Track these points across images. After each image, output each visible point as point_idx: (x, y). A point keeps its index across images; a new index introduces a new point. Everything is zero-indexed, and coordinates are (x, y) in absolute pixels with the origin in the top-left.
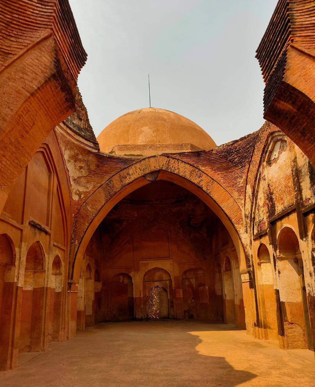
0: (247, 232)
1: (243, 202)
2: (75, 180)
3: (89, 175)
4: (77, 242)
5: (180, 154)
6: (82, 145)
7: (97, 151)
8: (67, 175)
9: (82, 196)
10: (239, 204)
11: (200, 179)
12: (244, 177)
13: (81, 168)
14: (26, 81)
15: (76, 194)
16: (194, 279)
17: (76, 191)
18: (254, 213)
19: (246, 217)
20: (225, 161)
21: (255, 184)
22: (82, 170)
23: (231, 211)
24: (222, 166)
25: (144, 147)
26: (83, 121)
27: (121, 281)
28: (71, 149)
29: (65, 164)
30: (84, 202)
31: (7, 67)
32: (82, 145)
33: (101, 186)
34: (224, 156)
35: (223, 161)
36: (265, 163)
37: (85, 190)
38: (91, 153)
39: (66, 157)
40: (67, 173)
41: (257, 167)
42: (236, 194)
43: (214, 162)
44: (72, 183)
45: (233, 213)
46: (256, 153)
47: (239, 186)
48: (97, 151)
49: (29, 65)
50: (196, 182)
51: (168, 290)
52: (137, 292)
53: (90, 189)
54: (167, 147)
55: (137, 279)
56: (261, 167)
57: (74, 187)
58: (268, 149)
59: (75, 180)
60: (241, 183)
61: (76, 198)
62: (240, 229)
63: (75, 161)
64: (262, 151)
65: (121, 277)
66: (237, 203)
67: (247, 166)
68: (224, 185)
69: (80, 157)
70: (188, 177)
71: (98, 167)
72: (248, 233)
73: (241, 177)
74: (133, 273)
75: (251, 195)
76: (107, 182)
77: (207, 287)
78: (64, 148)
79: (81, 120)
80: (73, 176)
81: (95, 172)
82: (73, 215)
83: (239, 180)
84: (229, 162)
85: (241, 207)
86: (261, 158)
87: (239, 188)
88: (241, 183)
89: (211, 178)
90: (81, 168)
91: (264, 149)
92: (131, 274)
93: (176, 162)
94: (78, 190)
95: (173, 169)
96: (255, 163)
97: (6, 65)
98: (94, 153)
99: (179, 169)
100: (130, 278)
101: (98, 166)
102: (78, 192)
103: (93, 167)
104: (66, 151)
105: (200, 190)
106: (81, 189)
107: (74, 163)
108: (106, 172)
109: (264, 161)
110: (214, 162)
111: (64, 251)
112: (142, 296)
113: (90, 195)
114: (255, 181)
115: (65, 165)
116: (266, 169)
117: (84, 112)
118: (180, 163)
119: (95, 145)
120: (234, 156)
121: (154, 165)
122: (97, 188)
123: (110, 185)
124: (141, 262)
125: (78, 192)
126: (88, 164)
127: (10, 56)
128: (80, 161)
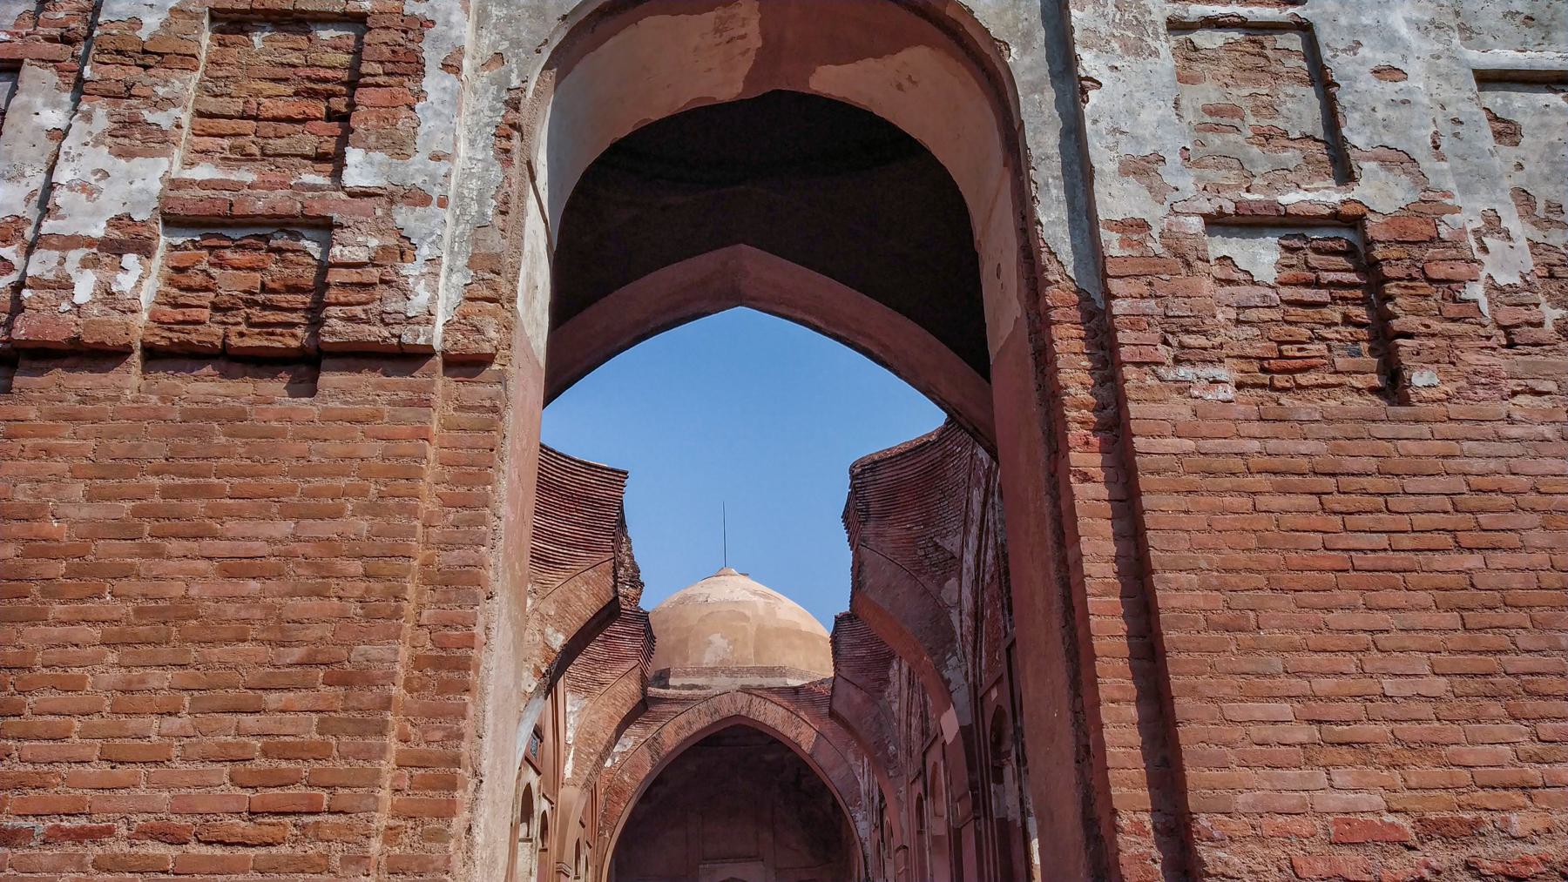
5: (769, 689)
25: (713, 671)
42: (851, 758)
50: (791, 735)
54: (749, 671)
68: (834, 741)
70: (780, 728)
108: (655, 719)
121: (727, 709)
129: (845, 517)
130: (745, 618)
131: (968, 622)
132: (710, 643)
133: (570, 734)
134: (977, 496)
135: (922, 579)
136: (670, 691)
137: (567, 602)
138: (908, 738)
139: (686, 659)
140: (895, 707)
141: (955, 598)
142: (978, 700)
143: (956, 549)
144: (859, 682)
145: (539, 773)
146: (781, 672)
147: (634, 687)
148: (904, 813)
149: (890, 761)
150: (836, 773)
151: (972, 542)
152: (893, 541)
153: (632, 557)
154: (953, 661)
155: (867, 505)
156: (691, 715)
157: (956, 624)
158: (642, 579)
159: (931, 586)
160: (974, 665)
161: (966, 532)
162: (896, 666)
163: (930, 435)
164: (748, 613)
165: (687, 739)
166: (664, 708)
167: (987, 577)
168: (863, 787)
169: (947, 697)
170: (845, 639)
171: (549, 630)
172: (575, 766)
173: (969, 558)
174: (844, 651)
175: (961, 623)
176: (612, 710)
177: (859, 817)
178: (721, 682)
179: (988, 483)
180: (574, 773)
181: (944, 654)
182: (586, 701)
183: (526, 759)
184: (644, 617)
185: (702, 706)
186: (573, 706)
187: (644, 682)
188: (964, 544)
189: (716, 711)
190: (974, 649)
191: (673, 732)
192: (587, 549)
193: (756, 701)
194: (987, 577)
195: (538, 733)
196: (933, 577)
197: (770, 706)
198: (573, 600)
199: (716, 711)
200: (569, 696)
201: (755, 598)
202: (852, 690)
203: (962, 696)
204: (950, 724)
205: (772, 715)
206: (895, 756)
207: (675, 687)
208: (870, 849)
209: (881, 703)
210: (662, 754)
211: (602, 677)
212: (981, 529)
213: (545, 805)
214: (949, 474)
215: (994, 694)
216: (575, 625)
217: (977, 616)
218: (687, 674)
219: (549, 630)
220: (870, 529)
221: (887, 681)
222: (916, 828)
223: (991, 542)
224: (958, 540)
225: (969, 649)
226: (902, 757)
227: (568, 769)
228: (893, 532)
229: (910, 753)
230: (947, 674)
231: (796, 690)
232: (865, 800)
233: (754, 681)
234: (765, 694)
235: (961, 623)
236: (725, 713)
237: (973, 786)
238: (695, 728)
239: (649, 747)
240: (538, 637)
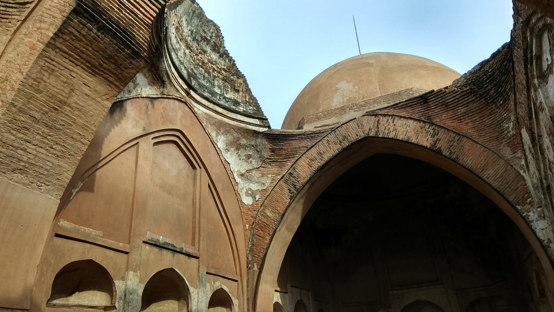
0: (544, 217)
1: (523, 162)
2: (242, 175)
3: (263, 166)
4: (256, 267)
6: (243, 125)
7: (266, 129)
8: (228, 169)
9: (258, 197)
10: (517, 168)
11: (435, 139)
12: (513, 118)
13: (249, 157)
14: (43, 31)
15: (247, 194)
17: (247, 191)
18: (546, 179)
19: (535, 188)
20: (473, 98)
21: (531, 124)
22: (251, 159)
23: (504, 183)
24: (469, 109)
25: (342, 110)
26: (241, 93)
28: (226, 132)
29: (220, 155)
30: (261, 206)
31: (24, 21)
32: (243, 125)
33: (282, 178)
34: (468, 91)
35: (470, 100)
36: (536, 81)
37: (260, 188)
38: (259, 133)
39: (221, 144)
40: (227, 166)
41: (525, 92)
42: (507, 152)
43: (453, 105)
44: (238, 180)
45: (507, 186)
46: (517, 69)
47: (509, 135)
48: (266, 129)
49: (47, 9)
53: (267, 185)
56: (532, 90)
57: (242, 185)
58: (532, 52)
59: (242, 175)
60: (510, 129)
61: (247, 201)
62: (529, 212)
63: (238, 149)
64: (524, 60)
66: (512, 166)
67: (512, 96)
68: (480, 140)
69: (244, 141)
70: (414, 140)
71: (273, 152)
72: (546, 217)
73: (509, 119)
75: (531, 146)
76: (290, 171)
78: (215, 132)
79: (238, 91)
80: (239, 171)
81: (270, 159)
82: (247, 226)
83: (507, 126)
84: (480, 99)
85: (522, 172)
86: (526, 74)
87: (510, 139)
88: (510, 129)
89: (454, 132)
90: (249, 157)
91: (525, 55)
93: (391, 120)
94: (250, 189)
95: (386, 132)
96: (521, 87)
97: (23, 18)
98: (263, 133)
99: (396, 130)
101: (273, 150)
102: (249, 192)
103: (266, 154)
104: (219, 137)
105: (440, 156)
106: (254, 187)
107: (236, 152)
108: (288, 157)
109: (533, 78)
110: (453, 105)
111: (236, 281)
113: (268, 194)
114: (531, 118)
115: (221, 157)
116: (539, 90)
117: (241, 81)
118: (395, 120)
119: (263, 122)
120: (486, 87)
121: (355, 134)
122: (277, 181)
123: (295, 174)
124: (391, 293)
125: (249, 192)
126: (258, 150)
127: (27, 6)
128: (245, 147)
132: (337, 90)
156: (321, 147)
166: (295, 144)
177: (532, 216)
185: (331, 137)
189: (345, 138)
197: (399, 122)
199: (345, 138)
205: (405, 129)
210: (298, 186)
218: (318, 118)
231: (425, 99)
232: (536, 195)
234: (391, 112)
236: (353, 138)
239: (286, 182)
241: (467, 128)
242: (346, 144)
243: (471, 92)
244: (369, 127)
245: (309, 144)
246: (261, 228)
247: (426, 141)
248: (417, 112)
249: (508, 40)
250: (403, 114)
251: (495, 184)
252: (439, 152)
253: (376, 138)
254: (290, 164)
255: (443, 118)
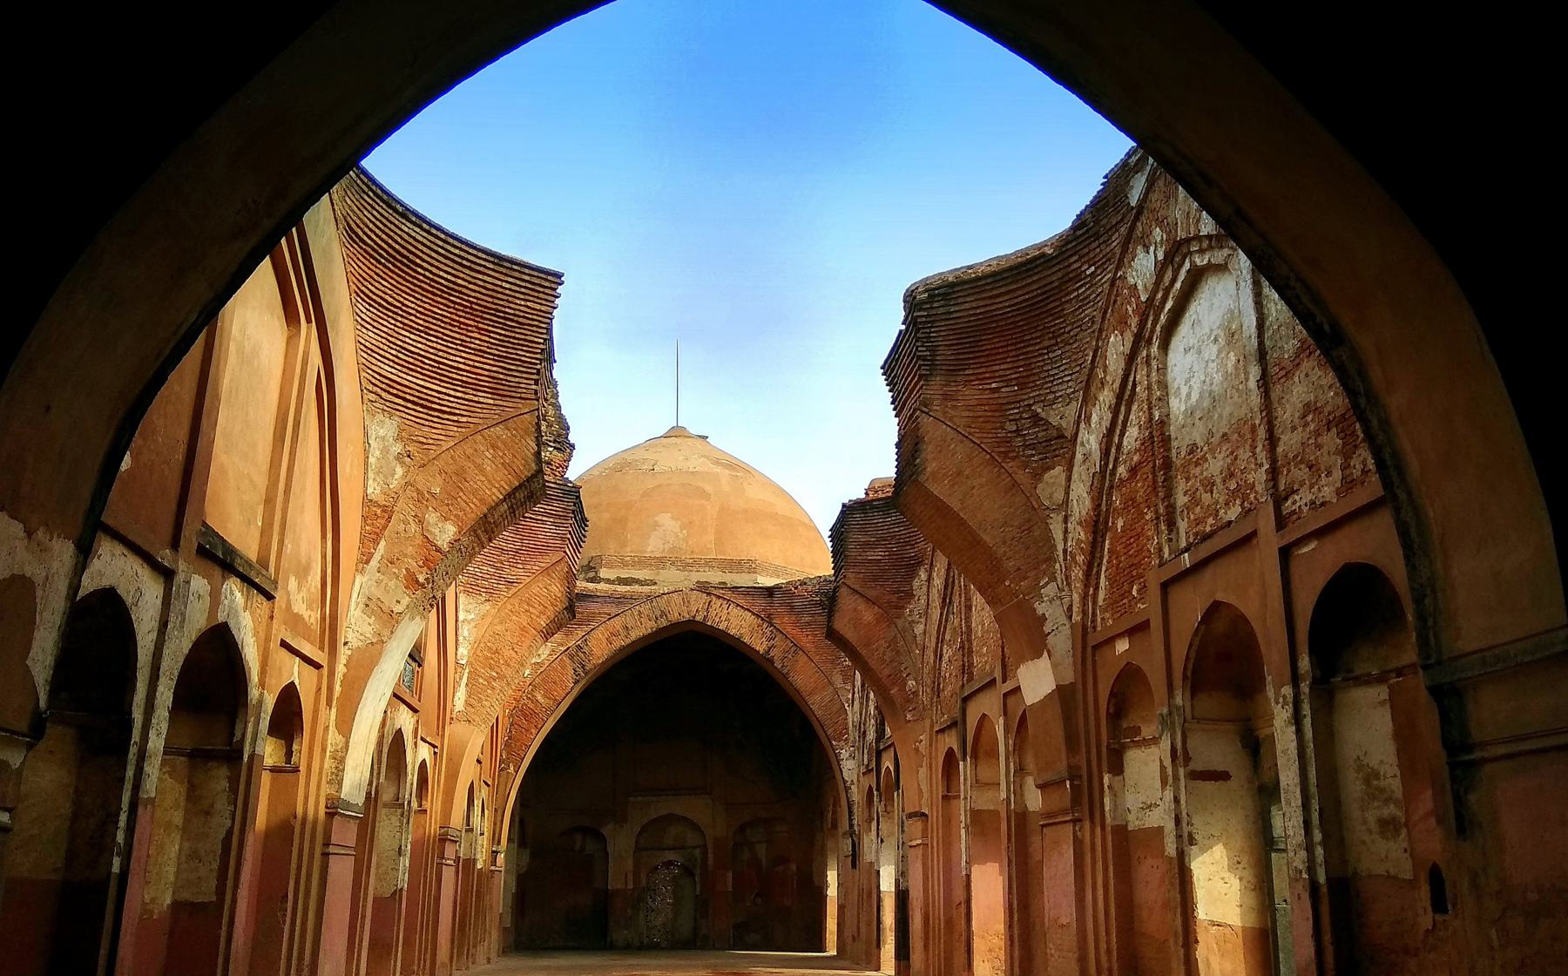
5: (735, 589)
16: (764, 846)
25: (660, 562)
27: (577, 847)
42: (838, 680)
51: (697, 872)
52: (619, 872)
54: (708, 564)
55: (621, 842)
65: (579, 838)
74: (610, 826)
77: (793, 867)
92: (607, 830)
100: (602, 839)
112: (630, 886)
123: (586, 649)
129: (892, 368)
130: (703, 494)
131: (1079, 534)
132: (656, 525)
133: (463, 651)
134: (1117, 346)
135: (1009, 465)
136: (602, 586)
137: (461, 473)
138: (937, 670)
139: (623, 545)
140: (919, 629)
141: (1059, 496)
142: (1089, 647)
143: (1067, 425)
144: (871, 593)
145: (415, 711)
146: (750, 566)
147: (557, 589)
148: (923, 771)
149: (908, 701)
150: (817, 698)
151: (1100, 415)
152: (968, 408)
153: (558, 407)
154: (1050, 590)
155: (933, 350)
157: (1058, 535)
158: (572, 438)
159: (1023, 477)
160: (1084, 598)
161: (1088, 399)
162: (923, 575)
163: (1044, 245)
164: (708, 488)
165: (622, 649)
166: (594, 607)
167: (1122, 470)
168: (853, 715)
169: (1036, 644)
170: (855, 537)
171: (432, 517)
172: (469, 695)
173: (1090, 440)
174: (853, 551)
175: (1067, 535)
176: (524, 620)
177: (844, 754)
178: (670, 578)
179: (1142, 324)
180: (468, 704)
181: (1038, 579)
182: (487, 606)
183: (395, 695)
184: (572, 493)
185: (645, 608)
186: (470, 615)
187: (570, 578)
188: (1083, 417)
189: (663, 614)
190: (1088, 574)
191: (603, 642)
192: (494, 392)
193: (717, 603)
194: (1122, 470)
195: (416, 656)
196: (1025, 465)
197: (735, 611)
198: (472, 471)
199: (663, 614)
200: (462, 598)
201: (718, 470)
202: (862, 606)
203: (1061, 640)
204: (1037, 681)
205: (737, 622)
206: (916, 693)
207: (608, 581)
208: (856, 795)
209: (900, 622)
211: (511, 573)
212: (1119, 397)
213: (424, 752)
214: (1069, 309)
215: (1122, 646)
216: (475, 510)
217: (1098, 526)
218: (624, 564)
219: (432, 517)
220: (935, 388)
221: (910, 595)
222: (940, 792)
223: (1137, 415)
224: (1072, 410)
225: (1078, 573)
226: (924, 698)
227: (459, 699)
228: (970, 394)
229: (937, 692)
230: (1041, 609)
231: (769, 592)
232: (853, 734)
233: (714, 577)
234: (728, 595)
235: (1067, 535)
236: (674, 617)
237: (1074, 775)
238: (635, 635)
239: (571, 657)
240: (413, 527)
241: (806, 641)
242: (663, 623)
243: (821, 604)
244: (696, 608)
245: (614, 611)
246: (525, 716)
247: (760, 645)
248: (760, 603)
249: (886, 467)
250: (741, 602)
251: (819, 713)
252: (771, 661)
253: (702, 624)
254: (581, 633)
255: (784, 621)
